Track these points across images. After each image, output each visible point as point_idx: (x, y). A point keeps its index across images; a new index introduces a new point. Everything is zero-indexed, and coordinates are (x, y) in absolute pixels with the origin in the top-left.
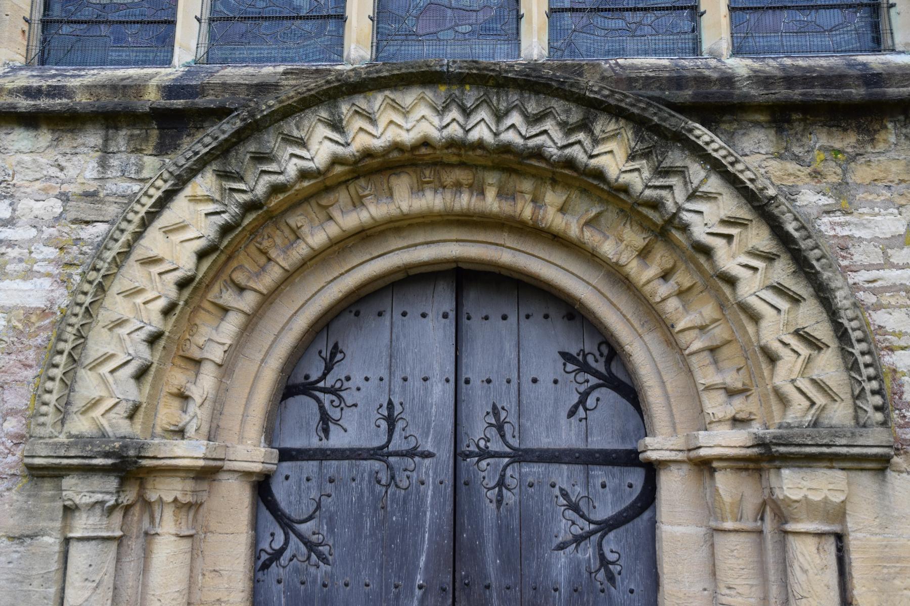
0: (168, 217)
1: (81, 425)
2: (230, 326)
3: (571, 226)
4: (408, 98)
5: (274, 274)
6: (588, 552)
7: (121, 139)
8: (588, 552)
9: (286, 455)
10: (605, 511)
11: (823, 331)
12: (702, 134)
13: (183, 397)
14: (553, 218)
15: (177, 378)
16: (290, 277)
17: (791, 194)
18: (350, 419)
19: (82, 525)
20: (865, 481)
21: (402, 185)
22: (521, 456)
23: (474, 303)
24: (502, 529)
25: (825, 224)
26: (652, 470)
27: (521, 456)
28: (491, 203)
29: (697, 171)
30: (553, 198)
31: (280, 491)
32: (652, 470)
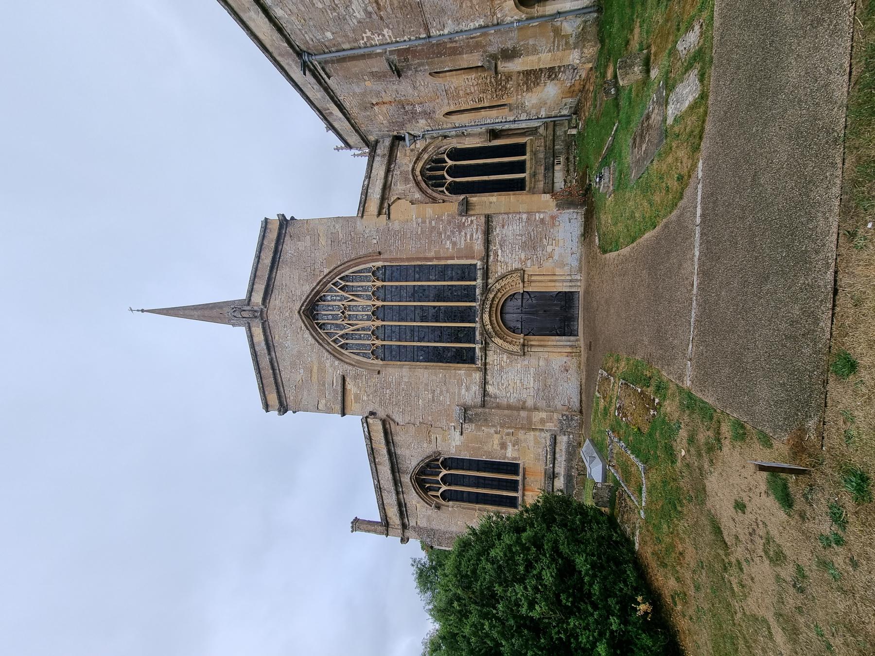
0: (497, 343)
1: (519, 351)
2: (508, 337)
3: (497, 300)
4: (484, 318)
5: (502, 333)
6: (533, 299)
7: (488, 349)
8: (533, 299)
9: (522, 333)
10: (529, 297)
11: (511, 275)
12: (489, 286)
13: (516, 342)
14: (496, 303)
15: (514, 343)
16: (502, 331)
17: (496, 278)
18: (517, 326)
19: (529, 350)
20: (526, 272)
21: (492, 319)
22: (522, 306)
23: (504, 312)
24: (530, 308)
25: (499, 274)
26: (524, 291)
27: (522, 306)
28: (494, 309)
29: (493, 287)
30: (494, 302)
31: (526, 334)
32: (524, 291)
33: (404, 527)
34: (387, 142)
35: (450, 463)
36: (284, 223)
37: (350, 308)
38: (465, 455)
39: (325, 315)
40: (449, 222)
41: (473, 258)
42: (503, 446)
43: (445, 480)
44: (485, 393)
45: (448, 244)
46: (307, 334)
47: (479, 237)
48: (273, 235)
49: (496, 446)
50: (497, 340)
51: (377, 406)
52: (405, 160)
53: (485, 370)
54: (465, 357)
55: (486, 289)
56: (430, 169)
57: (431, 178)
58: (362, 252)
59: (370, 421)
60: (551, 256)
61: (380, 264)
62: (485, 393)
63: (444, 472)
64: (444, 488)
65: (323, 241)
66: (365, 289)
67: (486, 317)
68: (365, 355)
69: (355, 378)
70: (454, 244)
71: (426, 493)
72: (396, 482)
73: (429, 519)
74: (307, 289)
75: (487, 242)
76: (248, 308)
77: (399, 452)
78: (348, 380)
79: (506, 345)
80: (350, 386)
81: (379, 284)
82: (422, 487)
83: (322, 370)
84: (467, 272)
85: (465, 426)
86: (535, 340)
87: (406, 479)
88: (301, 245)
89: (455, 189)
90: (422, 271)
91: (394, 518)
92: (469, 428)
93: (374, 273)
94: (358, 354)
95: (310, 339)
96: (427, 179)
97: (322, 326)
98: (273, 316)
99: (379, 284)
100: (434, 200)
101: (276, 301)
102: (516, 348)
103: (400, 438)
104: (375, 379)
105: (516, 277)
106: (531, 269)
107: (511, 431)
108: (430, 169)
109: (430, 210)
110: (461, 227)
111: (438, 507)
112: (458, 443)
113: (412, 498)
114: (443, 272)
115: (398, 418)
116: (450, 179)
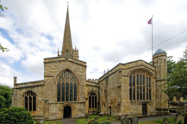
33: (17, 89)
34: (99, 86)
35: (35, 98)
36: (86, 67)
37: (68, 78)
38: (37, 101)
39: (67, 73)
40: (84, 96)
41: (78, 100)
42: (40, 108)
43: (30, 97)
44: (51, 104)
45: (80, 96)
46: (63, 69)
47: (81, 101)
48: (83, 64)
49: (39, 106)
50: (62, 105)
51: (47, 83)
52: (95, 89)
53: (56, 103)
54: (59, 100)
55: (72, 103)
56: (94, 93)
57: (92, 93)
58: (79, 81)
59: (43, 82)
60: (78, 113)
61: (77, 84)
62: (51, 104)
63: (32, 97)
64: (28, 97)
65: (82, 74)
66: (72, 81)
67: (67, 103)
68: (58, 81)
69: (53, 79)
70: (80, 97)
71: (26, 93)
72: (29, 87)
73: (20, 94)
74: (72, 70)
75: (80, 103)
76: (68, 58)
77: (36, 88)
78: (53, 77)
79: (61, 107)
80: (51, 78)
81: (73, 84)
82: (28, 92)
83: (55, 72)
84: (75, 99)
85: (44, 101)
86: (62, 112)
87: (30, 89)
88: (81, 69)
89: (90, 97)
90: (75, 92)
91: (18, 87)
92: (43, 101)
93: (75, 83)
94: (59, 79)
95: (62, 70)
96: (92, 92)
97: (64, 72)
98: (67, 62)
99: (73, 84)
100: (88, 94)
101: (70, 64)
102: (61, 109)
103: (40, 88)
104: (53, 83)
105: (74, 108)
106: (75, 110)
107: (43, 109)
108: (94, 93)
109: (86, 93)
110: (83, 98)
111: (23, 96)
112: (40, 99)
113: (24, 91)
114: (75, 95)
115: (44, 87)
116: (92, 96)
